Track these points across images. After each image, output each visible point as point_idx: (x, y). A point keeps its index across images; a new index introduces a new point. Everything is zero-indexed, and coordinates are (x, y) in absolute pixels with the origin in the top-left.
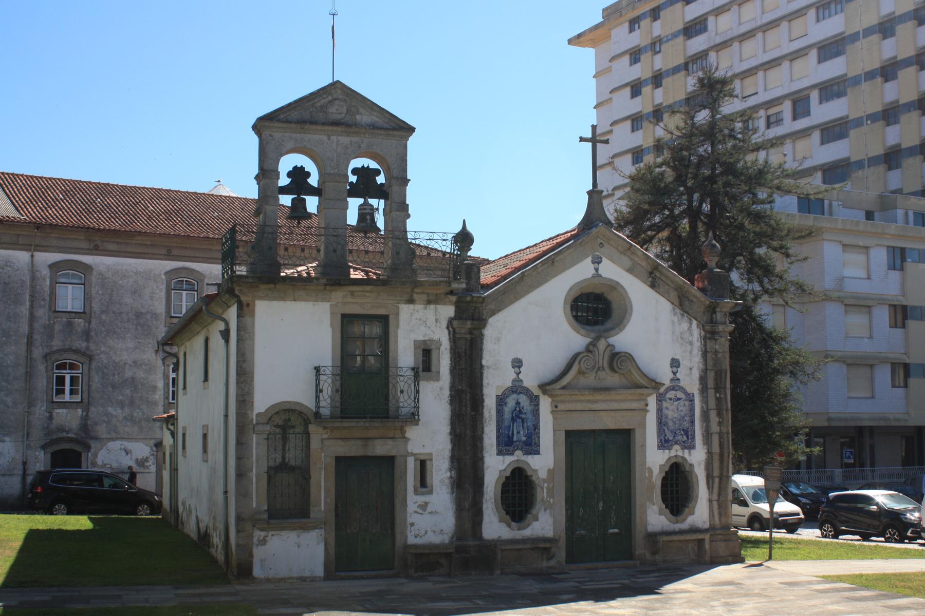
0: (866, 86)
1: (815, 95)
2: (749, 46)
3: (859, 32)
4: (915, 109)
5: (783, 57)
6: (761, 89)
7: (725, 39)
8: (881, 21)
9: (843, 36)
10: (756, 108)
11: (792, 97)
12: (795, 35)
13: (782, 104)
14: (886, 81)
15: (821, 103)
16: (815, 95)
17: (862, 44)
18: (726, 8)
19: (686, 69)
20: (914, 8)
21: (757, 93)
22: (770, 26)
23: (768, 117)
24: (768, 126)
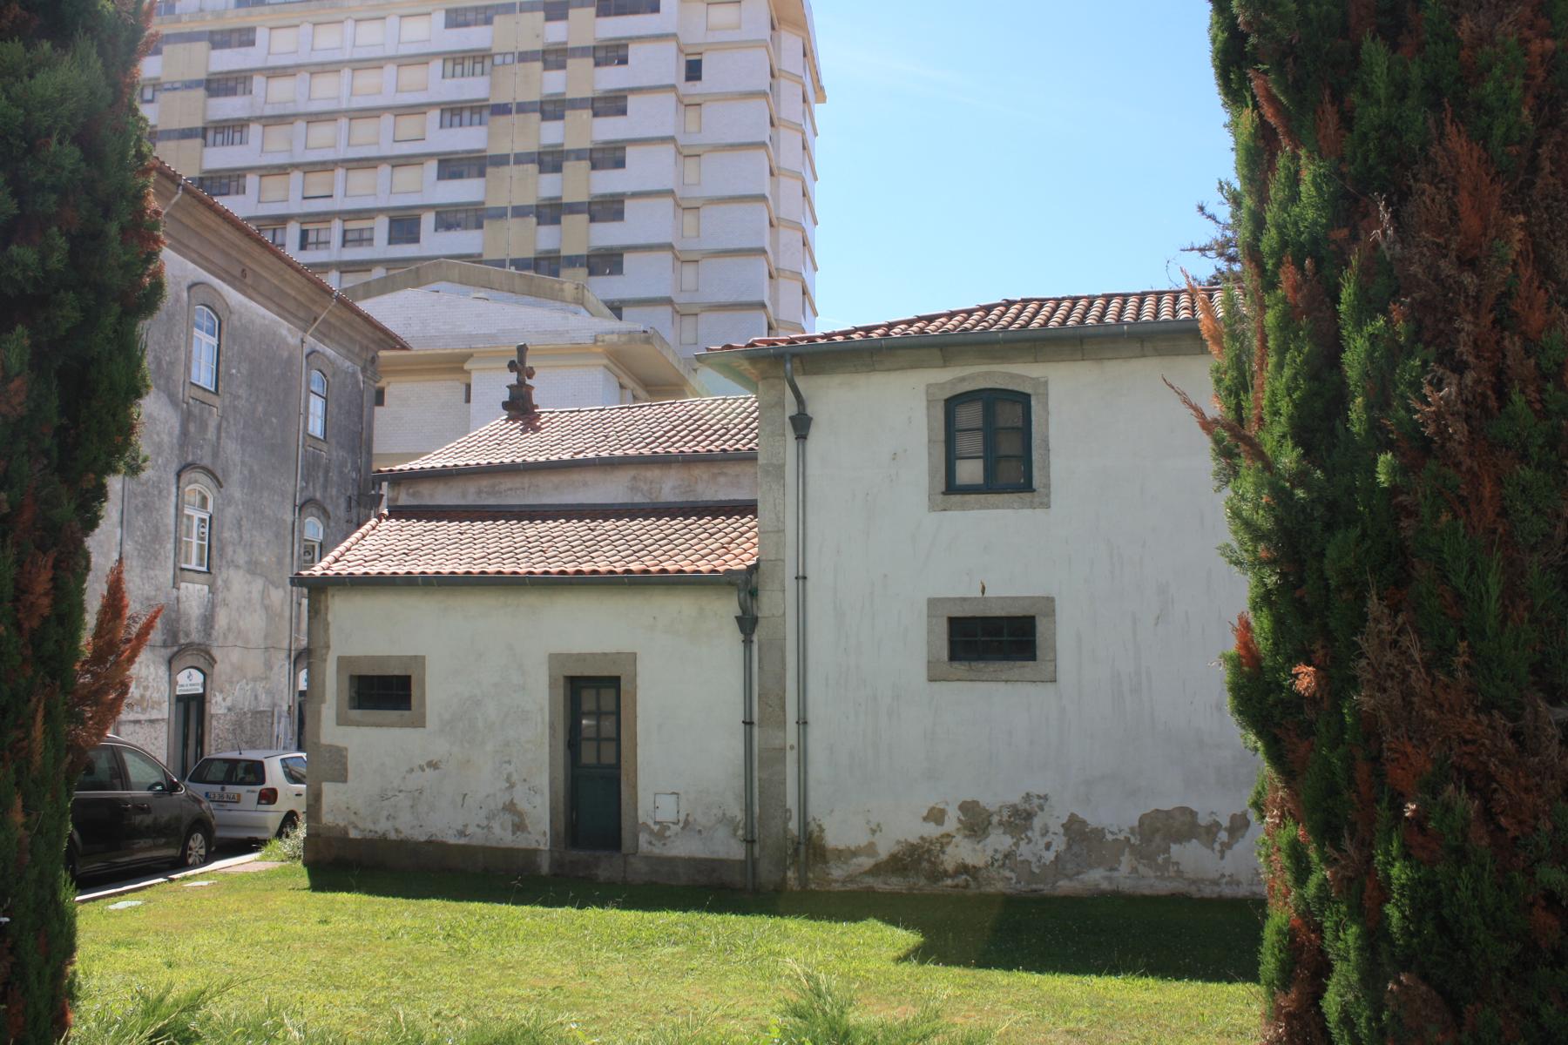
0: (513, 224)
1: (428, 220)
2: (322, 132)
3: (508, 155)
4: (581, 266)
5: (383, 159)
6: (338, 191)
7: (282, 112)
8: (541, 150)
9: (484, 154)
10: (325, 217)
11: (392, 214)
12: (400, 135)
13: (373, 218)
14: (539, 224)
15: (436, 230)
16: (428, 220)
17: (512, 170)
18: (290, 71)
19: (204, 137)
20: (591, 146)
21: (331, 196)
22: (364, 114)
23: (345, 232)
24: (345, 243)
